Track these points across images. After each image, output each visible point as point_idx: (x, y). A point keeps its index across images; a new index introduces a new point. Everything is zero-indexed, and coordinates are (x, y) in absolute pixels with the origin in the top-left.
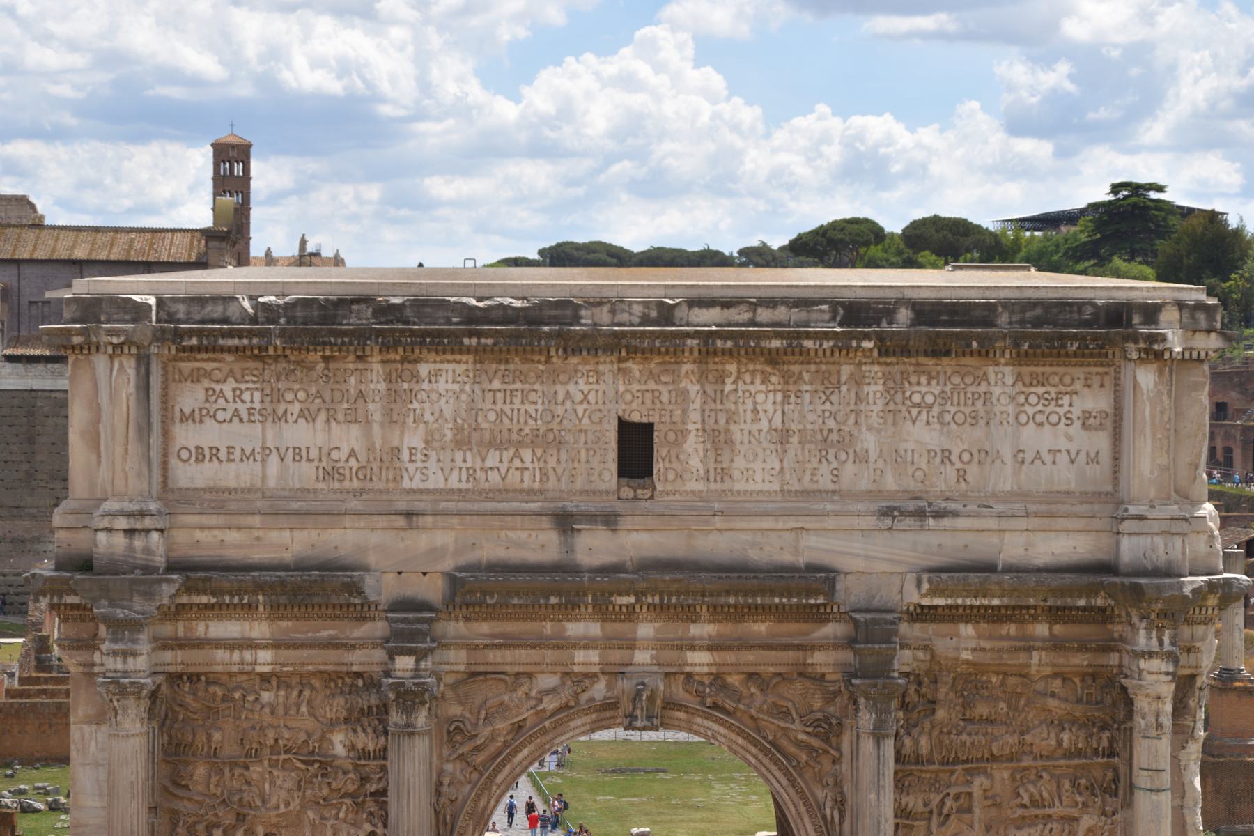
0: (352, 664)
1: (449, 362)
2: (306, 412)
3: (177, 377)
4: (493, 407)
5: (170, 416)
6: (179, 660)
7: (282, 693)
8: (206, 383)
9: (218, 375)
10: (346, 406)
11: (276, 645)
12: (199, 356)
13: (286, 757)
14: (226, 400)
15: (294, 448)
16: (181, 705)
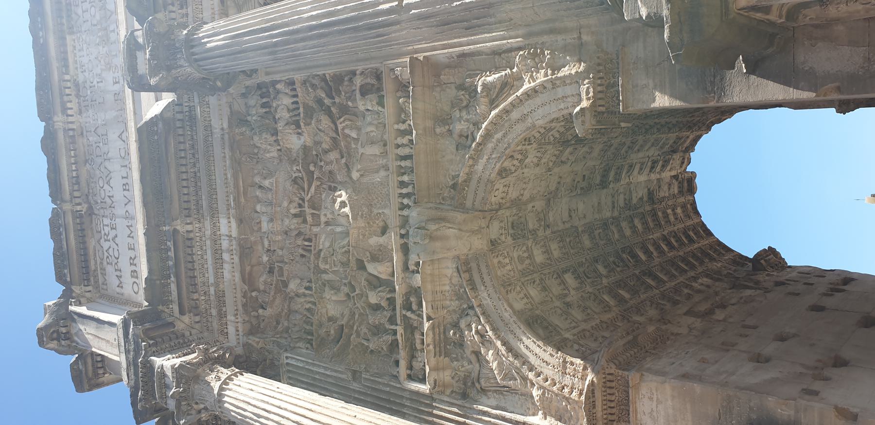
0: (222, 129)
1: (75, 56)
2: (108, 178)
3: (105, 287)
4: (89, 11)
5: (121, 297)
6: (233, 318)
7: (258, 208)
8: (105, 263)
9: (100, 252)
10: (101, 143)
11: (214, 213)
12: (93, 267)
13: (306, 203)
14: (110, 247)
15: (124, 190)
16: (278, 323)
